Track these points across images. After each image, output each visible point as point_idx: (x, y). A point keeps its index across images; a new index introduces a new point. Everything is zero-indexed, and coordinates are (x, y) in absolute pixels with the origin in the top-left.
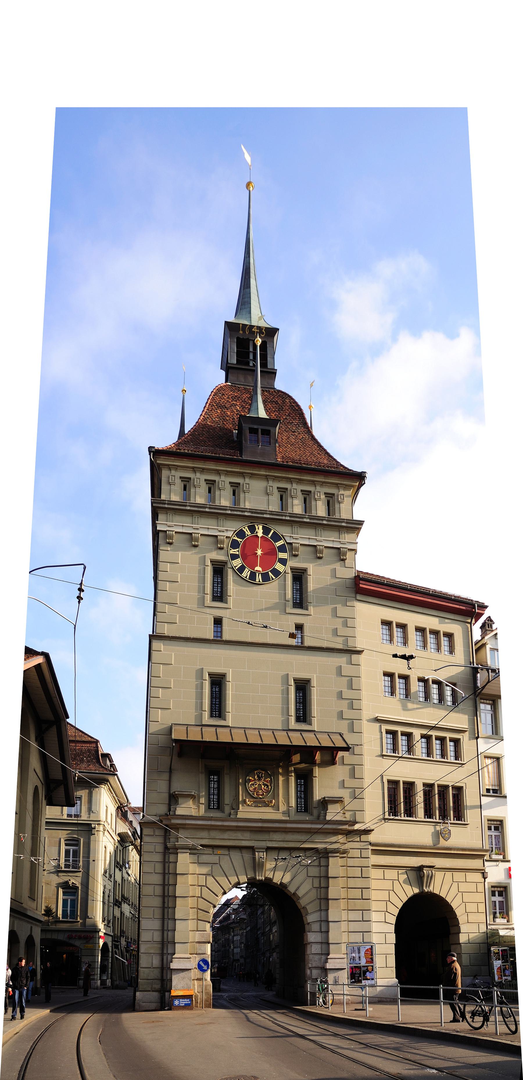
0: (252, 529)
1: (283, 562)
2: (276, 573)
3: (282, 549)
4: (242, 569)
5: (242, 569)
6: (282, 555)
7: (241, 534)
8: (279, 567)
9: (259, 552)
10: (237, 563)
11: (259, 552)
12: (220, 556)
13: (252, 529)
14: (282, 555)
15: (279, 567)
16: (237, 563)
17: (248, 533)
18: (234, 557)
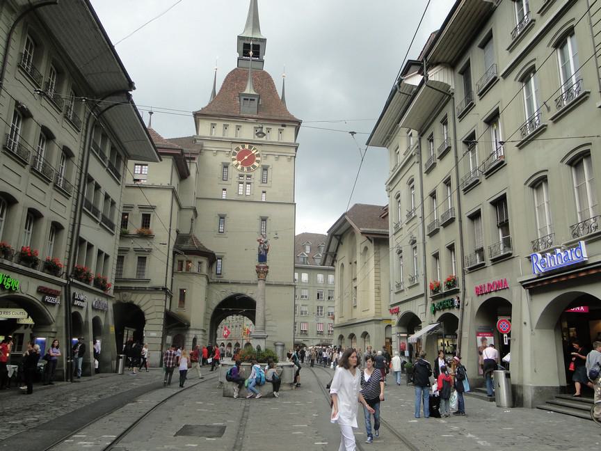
0: (243, 147)
1: (258, 162)
2: (254, 167)
3: (258, 155)
4: (237, 165)
5: (237, 165)
6: (257, 159)
7: (238, 149)
8: (256, 164)
9: (246, 158)
10: (235, 162)
11: (246, 158)
12: (227, 160)
13: (243, 147)
14: (257, 159)
15: (256, 164)
16: (235, 162)
17: (241, 148)
18: (234, 160)
